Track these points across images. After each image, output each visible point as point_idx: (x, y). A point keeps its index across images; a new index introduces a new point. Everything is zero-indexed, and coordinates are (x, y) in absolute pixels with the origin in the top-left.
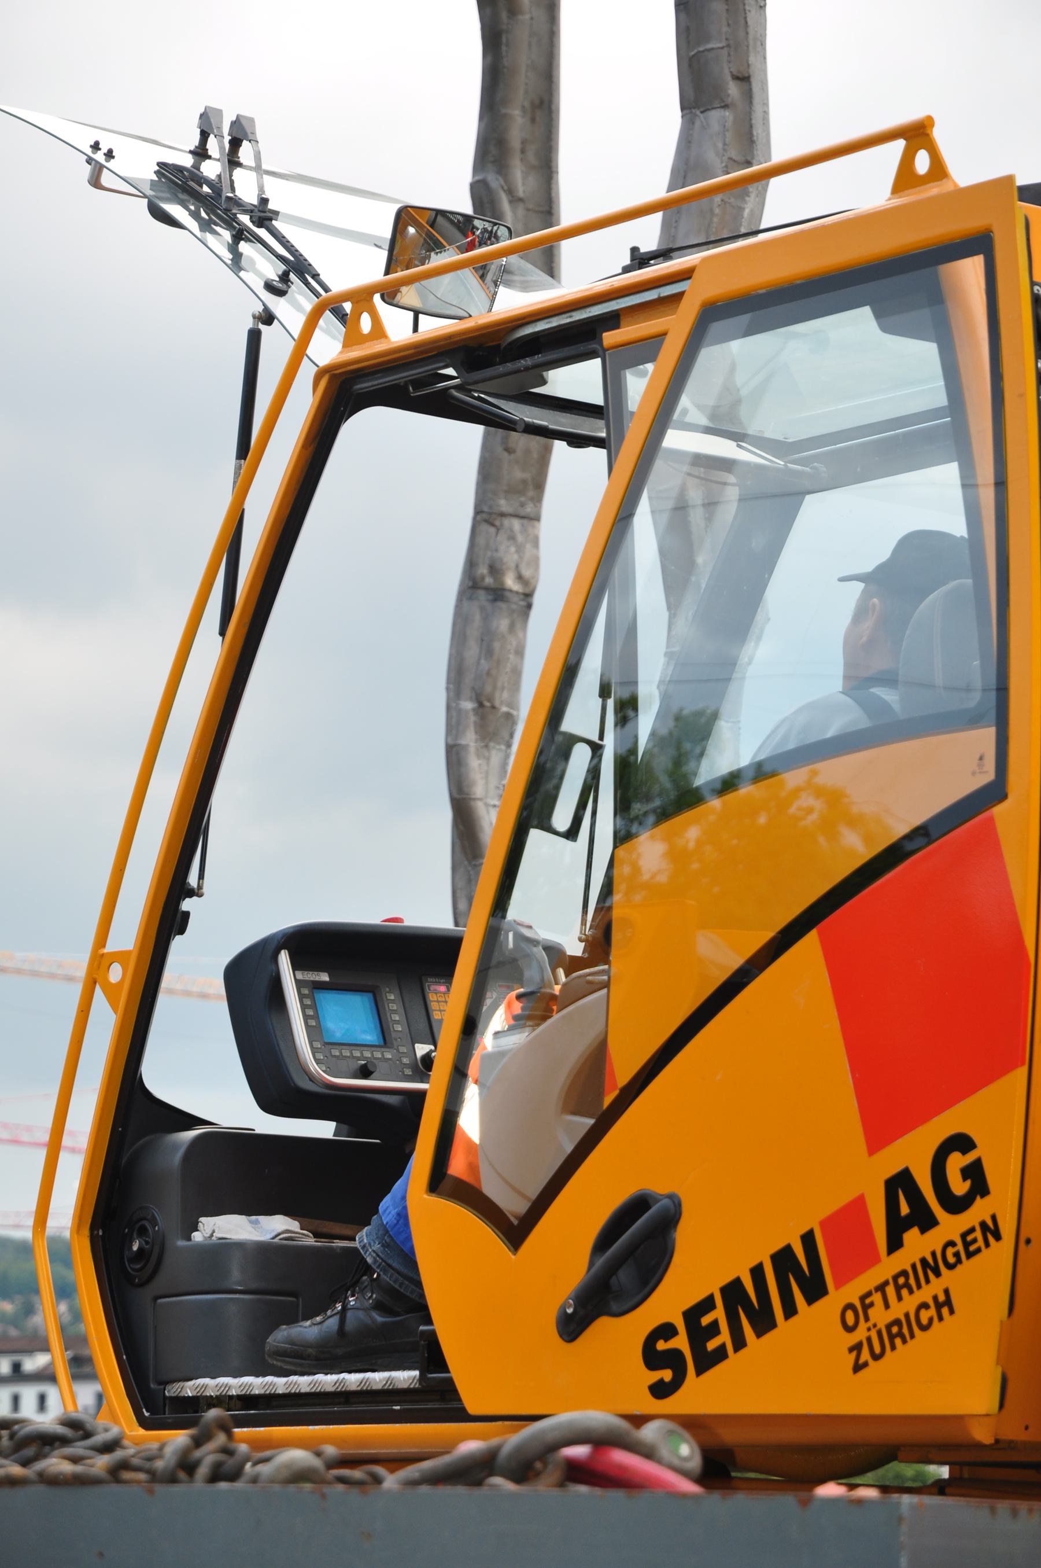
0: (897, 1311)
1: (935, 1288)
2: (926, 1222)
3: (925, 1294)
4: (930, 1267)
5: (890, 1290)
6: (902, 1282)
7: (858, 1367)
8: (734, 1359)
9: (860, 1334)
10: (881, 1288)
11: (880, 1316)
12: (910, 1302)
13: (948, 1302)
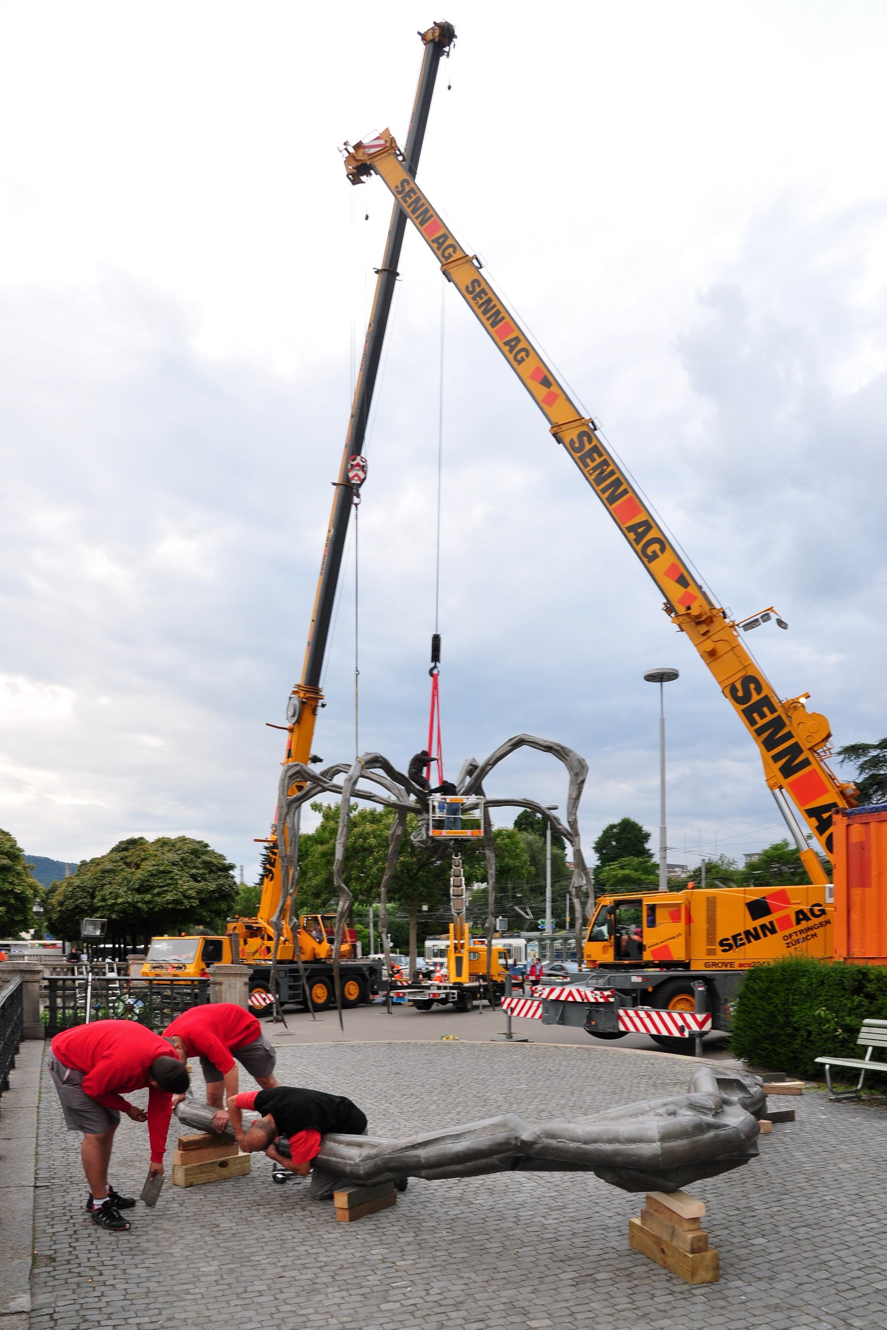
0: (800, 936)
1: (812, 932)
2: (807, 919)
3: (809, 933)
4: (809, 929)
5: (798, 933)
6: (801, 932)
7: (788, 947)
8: (748, 945)
9: (789, 941)
10: (795, 933)
11: (795, 937)
12: (804, 935)
13: (815, 935)
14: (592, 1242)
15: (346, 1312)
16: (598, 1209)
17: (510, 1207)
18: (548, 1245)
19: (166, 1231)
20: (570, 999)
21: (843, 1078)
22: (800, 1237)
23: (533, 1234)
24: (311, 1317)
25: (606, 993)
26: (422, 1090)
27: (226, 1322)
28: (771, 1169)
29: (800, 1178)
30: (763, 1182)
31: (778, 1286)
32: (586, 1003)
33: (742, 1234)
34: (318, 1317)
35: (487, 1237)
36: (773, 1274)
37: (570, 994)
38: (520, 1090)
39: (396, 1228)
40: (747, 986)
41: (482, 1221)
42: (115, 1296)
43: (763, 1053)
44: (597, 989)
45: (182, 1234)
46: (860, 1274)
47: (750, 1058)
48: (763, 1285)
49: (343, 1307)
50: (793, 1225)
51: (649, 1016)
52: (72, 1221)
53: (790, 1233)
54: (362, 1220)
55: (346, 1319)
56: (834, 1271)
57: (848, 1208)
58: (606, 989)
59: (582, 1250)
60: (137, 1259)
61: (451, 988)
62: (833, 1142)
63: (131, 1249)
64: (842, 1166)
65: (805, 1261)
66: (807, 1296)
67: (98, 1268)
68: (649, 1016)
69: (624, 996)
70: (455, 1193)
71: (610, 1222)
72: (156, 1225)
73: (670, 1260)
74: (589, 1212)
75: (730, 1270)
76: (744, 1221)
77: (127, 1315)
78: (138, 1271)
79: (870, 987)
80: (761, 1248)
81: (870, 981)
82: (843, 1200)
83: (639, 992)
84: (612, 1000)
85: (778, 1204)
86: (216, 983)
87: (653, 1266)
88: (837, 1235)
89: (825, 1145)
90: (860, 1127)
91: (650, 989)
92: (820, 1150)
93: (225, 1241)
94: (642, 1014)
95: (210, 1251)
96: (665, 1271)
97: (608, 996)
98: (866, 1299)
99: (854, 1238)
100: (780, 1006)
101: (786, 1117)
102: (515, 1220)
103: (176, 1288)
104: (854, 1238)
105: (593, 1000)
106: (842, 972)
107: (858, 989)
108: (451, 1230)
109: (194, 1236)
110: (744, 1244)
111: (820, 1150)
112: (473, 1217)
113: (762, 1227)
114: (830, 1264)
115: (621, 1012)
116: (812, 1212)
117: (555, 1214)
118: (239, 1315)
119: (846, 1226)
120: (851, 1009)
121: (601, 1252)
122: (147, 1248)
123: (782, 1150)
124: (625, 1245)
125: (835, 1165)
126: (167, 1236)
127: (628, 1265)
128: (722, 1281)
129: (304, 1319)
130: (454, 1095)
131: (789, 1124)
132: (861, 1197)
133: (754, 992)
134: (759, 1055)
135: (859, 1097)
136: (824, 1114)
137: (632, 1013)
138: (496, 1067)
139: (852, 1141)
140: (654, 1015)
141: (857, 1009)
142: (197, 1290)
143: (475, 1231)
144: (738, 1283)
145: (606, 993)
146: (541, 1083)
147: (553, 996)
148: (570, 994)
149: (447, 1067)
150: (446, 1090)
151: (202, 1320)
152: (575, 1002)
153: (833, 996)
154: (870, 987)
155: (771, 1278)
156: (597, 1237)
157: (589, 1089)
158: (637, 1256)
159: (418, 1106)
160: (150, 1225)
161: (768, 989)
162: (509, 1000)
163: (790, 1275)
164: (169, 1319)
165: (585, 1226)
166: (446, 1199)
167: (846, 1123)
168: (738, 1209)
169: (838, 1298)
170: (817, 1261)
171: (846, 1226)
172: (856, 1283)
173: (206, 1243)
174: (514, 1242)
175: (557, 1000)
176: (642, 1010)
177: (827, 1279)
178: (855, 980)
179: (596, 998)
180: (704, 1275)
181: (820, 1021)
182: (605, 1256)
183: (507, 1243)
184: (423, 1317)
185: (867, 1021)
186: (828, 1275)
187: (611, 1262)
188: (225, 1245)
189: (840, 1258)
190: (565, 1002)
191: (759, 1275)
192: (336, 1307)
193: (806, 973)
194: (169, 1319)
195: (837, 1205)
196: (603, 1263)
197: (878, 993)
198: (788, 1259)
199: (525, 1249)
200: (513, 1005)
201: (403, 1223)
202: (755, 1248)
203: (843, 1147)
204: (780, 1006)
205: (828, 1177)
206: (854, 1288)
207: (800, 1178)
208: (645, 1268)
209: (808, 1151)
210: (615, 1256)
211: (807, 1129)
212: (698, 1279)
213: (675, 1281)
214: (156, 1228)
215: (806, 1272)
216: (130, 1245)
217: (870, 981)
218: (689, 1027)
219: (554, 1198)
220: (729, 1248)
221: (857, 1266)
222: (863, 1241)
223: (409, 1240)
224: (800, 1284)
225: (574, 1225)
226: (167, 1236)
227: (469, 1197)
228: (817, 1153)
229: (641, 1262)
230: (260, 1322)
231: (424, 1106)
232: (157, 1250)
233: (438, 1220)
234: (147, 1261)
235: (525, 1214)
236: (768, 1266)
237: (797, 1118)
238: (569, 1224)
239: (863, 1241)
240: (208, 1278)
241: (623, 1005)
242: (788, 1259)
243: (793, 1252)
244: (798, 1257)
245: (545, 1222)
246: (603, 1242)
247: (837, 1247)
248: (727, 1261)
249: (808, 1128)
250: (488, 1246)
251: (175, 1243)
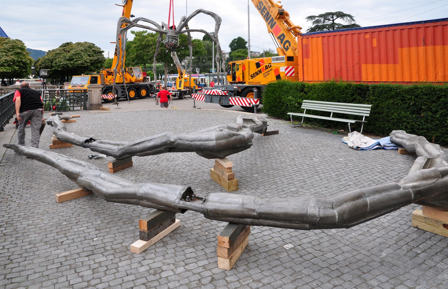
14: (198, 178)
15: (101, 207)
16: (203, 165)
17: (173, 166)
18: (182, 179)
19: (44, 180)
20: (214, 94)
21: (298, 120)
22: (270, 173)
23: (178, 175)
24: (86, 209)
25: (225, 92)
26: (155, 125)
27: (54, 213)
28: (266, 151)
29: (275, 153)
30: (262, 155)
31: (258, 191)
32: (219, 95)
33: (251, 173)
34: (89, 209)
35: (161, 177)
36: (257, 187)
37: (214, 92)
38: (189, 125)
39: (130, 175)
40: (267, 89)
41: (161, 171)
42: (14, 205)
43: (273, 112)
44: (222, 91)
45: (49, 181)
46: (287, 186)
47: (269, 113)
48: (254, 191)
49: (100, 205)
50: (268, 170)
51: (239, 100)
52: (8, 178)
53: (267, 172)
54: (118, 172)
55: (99, 209)
56: (279, 185)
57: (288, 163)
58: (225, 91)
59: (193, 180)
60: (28, 191)
62: (289, 141)
63: (27, 187)
64: (290, 149)
65: (269, 182)
66: (267, 194)
67: (11, 195)
68: (239, 100)
70: (155, 161)
71: (206, 170)
72: (41, 178)
73: (222, 183)
74: (200, 167)
75: (243, 186)
76: (252, 168)
77: (15, 212)
78: (27, 195)
79: (306, 90)
80: (256, 178)
81: (306, 88)
82: (287, 160)
84: (227, 94)
85: (265, 162)
86: (89, 91)
87: (216, 185)
88: (282, 173)
89: (286, 142)
90: (300, 136)
91: (240, 91)
92: (284, 143)
93: (65, 182)
94: (237, 99)
95: (58, 186)
96: (221, 187)
97: (226, 93)
98: (287, 194)
99: (288, 173)
100: (278, 96)
101: (276, 133)
102: (173, 170)
103: (39, 201)
104: (288, 173)
105: (221, 94)
106: (297, 85)
107: (302, 90)
108: (149, 175)
109: (54, 181)
110: (250, 176)
111: (284, 143)
112: (159, 170)
113: (258, 171)
114: (278, 183)
115: (230, 98)
116: (276, 165)
117: (188, 168)
118: (60, 210)
119: (286, 169)
120: (300, 97)
121: (200, 181)
122: (34, 187)
123: (272, 144)
124: (209, 178)
125: (288, 148)
126: (44, 181)
127: (208, 185)
128: (239, 190)
129: (84, 210)
130: (165, 127)
131: (276, 135)
132: (294, 159)
133: (270, 91)
134: (272, 112)
135: (302, 126)
136: (289, 132)
137: (234, 99)
138: (184, 117)
139: (296, 140)
140: (241, 99)
141: (302, 97)
142: (47, 201)
143: (158, 175)
144: (245, 191)
145: (225, 92)
146: (197, 122)
147: (208, 93)
148: (214, 92)
149: (167, 118)
150: (163, 125)
151: (45, 212)
152: (215, 95)
153: (294, 93)
154: (306, 90)
155: (256, 188)
156: (200, 176)
157: (213, 124)
158: (212, 182)
159: (152, 131)
160: (38, 178)
161: (274, 90)
162: (194, 95)
163: (263, 187)
164: (32, 213)
165: (197, 171)
166: (151, 163)
167: (295, 134)
168: (251, 164)
169: (277, 194)
170: (274, 182)
171: (286, 169)
172: (285, 189)
173: (57, 183)
174: (170, 178)
175: (209, 94)
176: (237, 97)
177: (276, 188)
178: (301, 87)
180: (232, 188)
181: (290, 101)
182: (201, 182)
183: (168, 179)
184: (128, 208)
185: (304, 101)
186: (276, 187)
187: (202, 184)
188: (64, 184)
189: (281, 181)
190: (212, 95)
191: (252, 187)
192: (98, 205)
193: (285, 85)
194: (32, 213)
195: (285, 162)
196: (199, 185)
197: (308, 92)
198: (264, 181)
199: (173, 181)
200: (195, 97)
201: (133, 173)
202: (253, 178)
203: (292, 142)
204: (278, 96)
205: (284, 153)
206: (284, 191)
207: (275, 153)
208: (214, 186)
209: (280, 144)
210: (205, 182)
211: (282, 137)
212: (231, 189)
213: (223, 191)
214: (40, 179)
215: (269, 186)
216: (27, 186)
217: (306, 88)
218: (252, 103)
219: (189, 162)
220: (245, 178)
221: (287, 183)
222: (291, 174)
223: (133, 179)
224: (266, 190)
225: (193, 171)
226: (44, 181)
227: (159, 163)
228: (283, 145)
229: (213, 184)
230: (66, 212)
231: (154, 131)
232: (38, 187)
233: (146, 171)
234: (32, 191)
235: (177, 168)
236: (257, 184)
237: (279, 133)
238: (192, 171)
239: (291, 174)
240: (53, 197)
241: (231, 96)
242: (264, 181)
243: (266, 179)
244: (268, 181)
245: (183, 171)
246: (202, 177)
247: (281, 177)
248: (243, 183)
249: (282, 136)
250: (160, 180)
251: (46, 184)
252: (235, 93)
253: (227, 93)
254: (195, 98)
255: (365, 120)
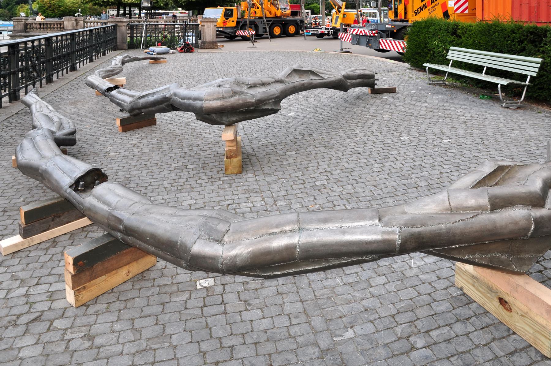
20: (361, 34)
25: (374, 32)
37: (361, 32)
44: (371, 30)
61: (331, 29)
69: (383, 33)
83: (389, 32)
84: (376, 35)
91: (395, 31)
94: (388, 41)
97: (375, 33)
105: (369, 35)
115: (380, 40)
137: (384, 41)
140: (393, 42)
145: (374, 32)
147: (354, 33)
148: (361, 32)
152: (363, 35)
162: (341, 34)
175: (356, 34)
179: (370, 34)
190: (359, 35)
200: (342, 36)
241: (381, 37)
252: (388, 34)
253: (377, 33)
254: (342, 38)
255: (529, 82)
